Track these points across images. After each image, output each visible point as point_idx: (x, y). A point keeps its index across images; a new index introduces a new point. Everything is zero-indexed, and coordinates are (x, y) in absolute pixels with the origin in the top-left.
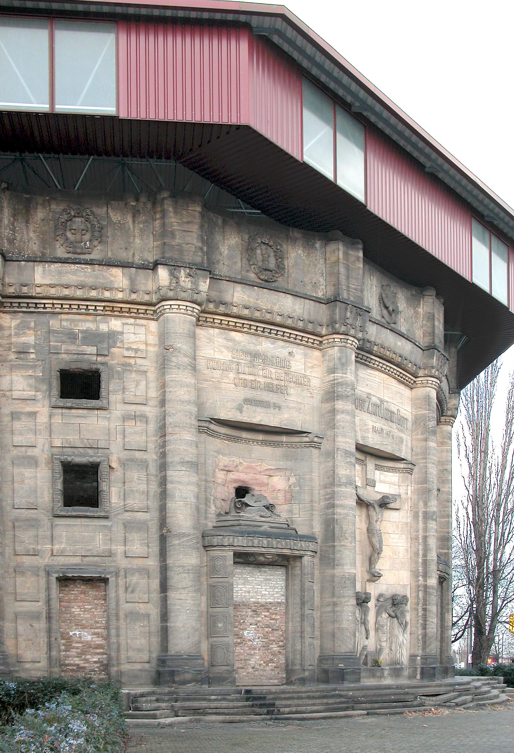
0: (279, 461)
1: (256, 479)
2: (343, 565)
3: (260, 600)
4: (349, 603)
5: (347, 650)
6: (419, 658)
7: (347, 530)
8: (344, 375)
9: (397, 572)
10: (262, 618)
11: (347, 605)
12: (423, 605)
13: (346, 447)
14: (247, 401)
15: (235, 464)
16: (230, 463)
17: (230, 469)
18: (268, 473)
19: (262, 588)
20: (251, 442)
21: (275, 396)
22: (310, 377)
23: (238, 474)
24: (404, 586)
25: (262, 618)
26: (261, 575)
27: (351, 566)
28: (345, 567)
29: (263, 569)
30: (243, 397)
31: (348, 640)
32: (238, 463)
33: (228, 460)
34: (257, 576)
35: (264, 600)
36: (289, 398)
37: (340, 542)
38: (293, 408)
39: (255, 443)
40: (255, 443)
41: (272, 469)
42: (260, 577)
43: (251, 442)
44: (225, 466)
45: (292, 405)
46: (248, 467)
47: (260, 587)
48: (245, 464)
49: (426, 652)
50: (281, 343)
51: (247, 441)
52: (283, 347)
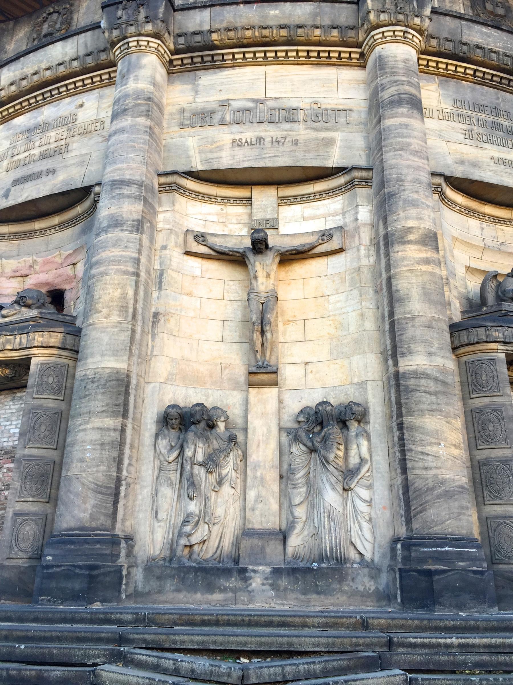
0: (77, 240)
1: (60, 276)
2: (86, 358)
3: (5, 444)
4: (89, 426)
5: (73, 524)
6: (399, 546)
7: (100, 298)
8: (123, 87)
9: (346, 362)
10: (3, 473)
11: (85, 430)
12: (397, 418)
13: (114, 176)
14: (16, 182)
15: (28, 264)
16: (20, 265)
17: (24, 272)
18: (69, 261)
19: (11, 425)
20: (48, 232)
21: (50, 161)
22: (102, 120)
23: (37, 275)
24: (362, 385)
25: (3, 473)
26: (13, 405)
27: (102, 355)
28: (90, 360)
29: (19, 395)
30: (12, 180)
31: (78, 502)
32: (31, 262)
33: (16, 262)
34: (8, 407)
35: (11, 444)
36: (70, 155)
37: (88, 320)
38: (74, 164)
39: (53, 230)
40: (53, 230)
41: (70, 255)
42: (12, 407)
43: (48, 232)
44: (15, 271)
45: (73, 162)
46: (46, 263)
47: (8, 423)
48: (39, 260)
49: (412, 531)
50: (68, 100)
51: (42, 232)
52: (69, 103)
